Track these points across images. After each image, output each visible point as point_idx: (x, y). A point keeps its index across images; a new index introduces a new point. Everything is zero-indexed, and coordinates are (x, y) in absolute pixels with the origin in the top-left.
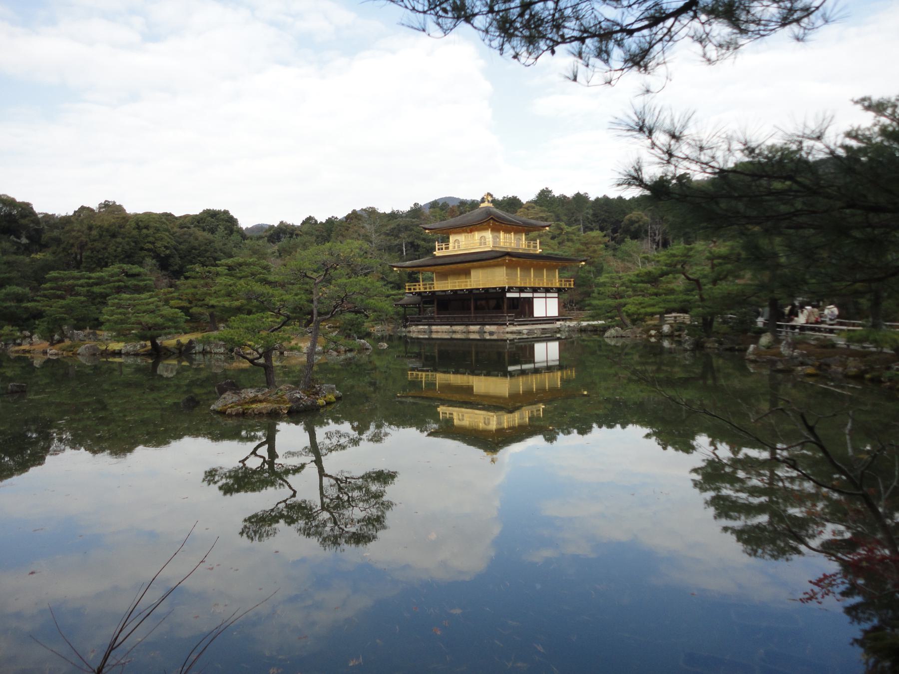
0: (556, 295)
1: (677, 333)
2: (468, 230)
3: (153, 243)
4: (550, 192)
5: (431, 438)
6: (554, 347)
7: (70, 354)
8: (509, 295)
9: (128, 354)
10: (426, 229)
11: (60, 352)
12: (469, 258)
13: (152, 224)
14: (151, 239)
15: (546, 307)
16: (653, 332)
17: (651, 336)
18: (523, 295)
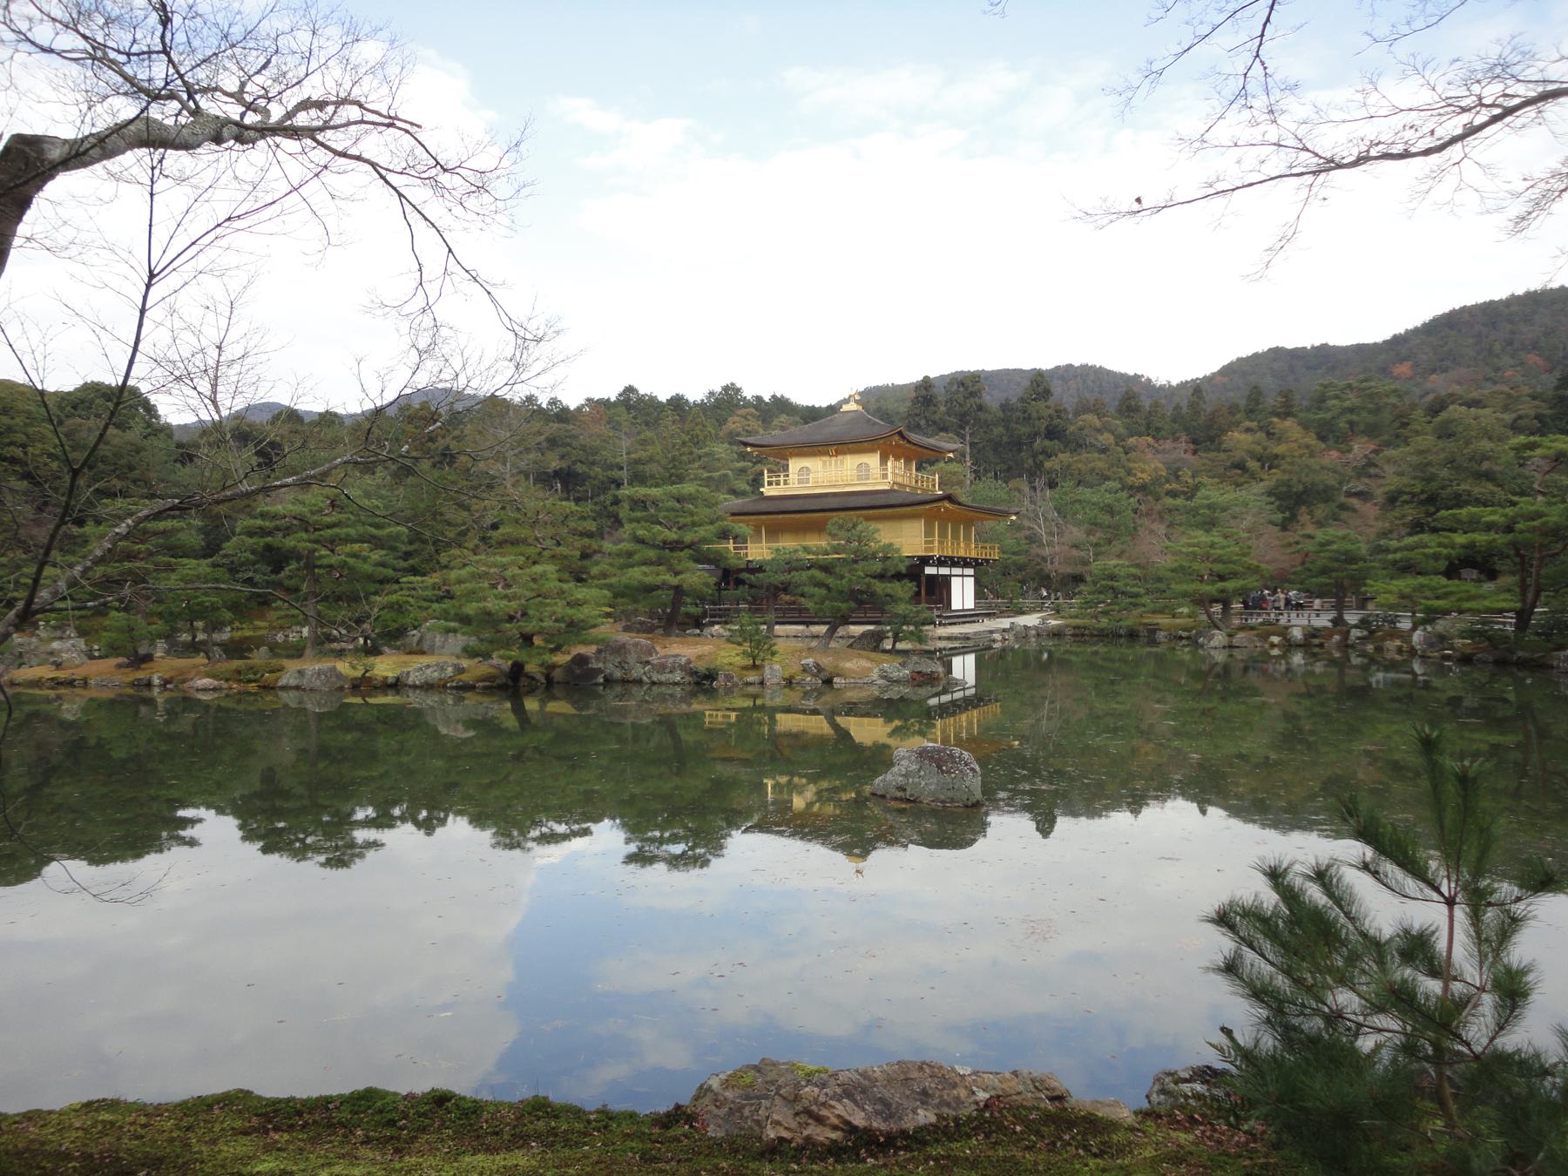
0: (971, 571)
1: (1316, 641)
2: (832, 450)
3: (24, 446)
4: (739, 390)
5: (747, 836)
6: (971, 659)
7: (252, 687)
8: (930, 570)
9: (427, 687)
10: (746, 444)
11: (225, 685)
12: (853, 502)
13: (20, 405)
14: (20, 438)
15: (963, 593)
16: (1275, 639)
17: (1273, 646)
18: (944, 571)
